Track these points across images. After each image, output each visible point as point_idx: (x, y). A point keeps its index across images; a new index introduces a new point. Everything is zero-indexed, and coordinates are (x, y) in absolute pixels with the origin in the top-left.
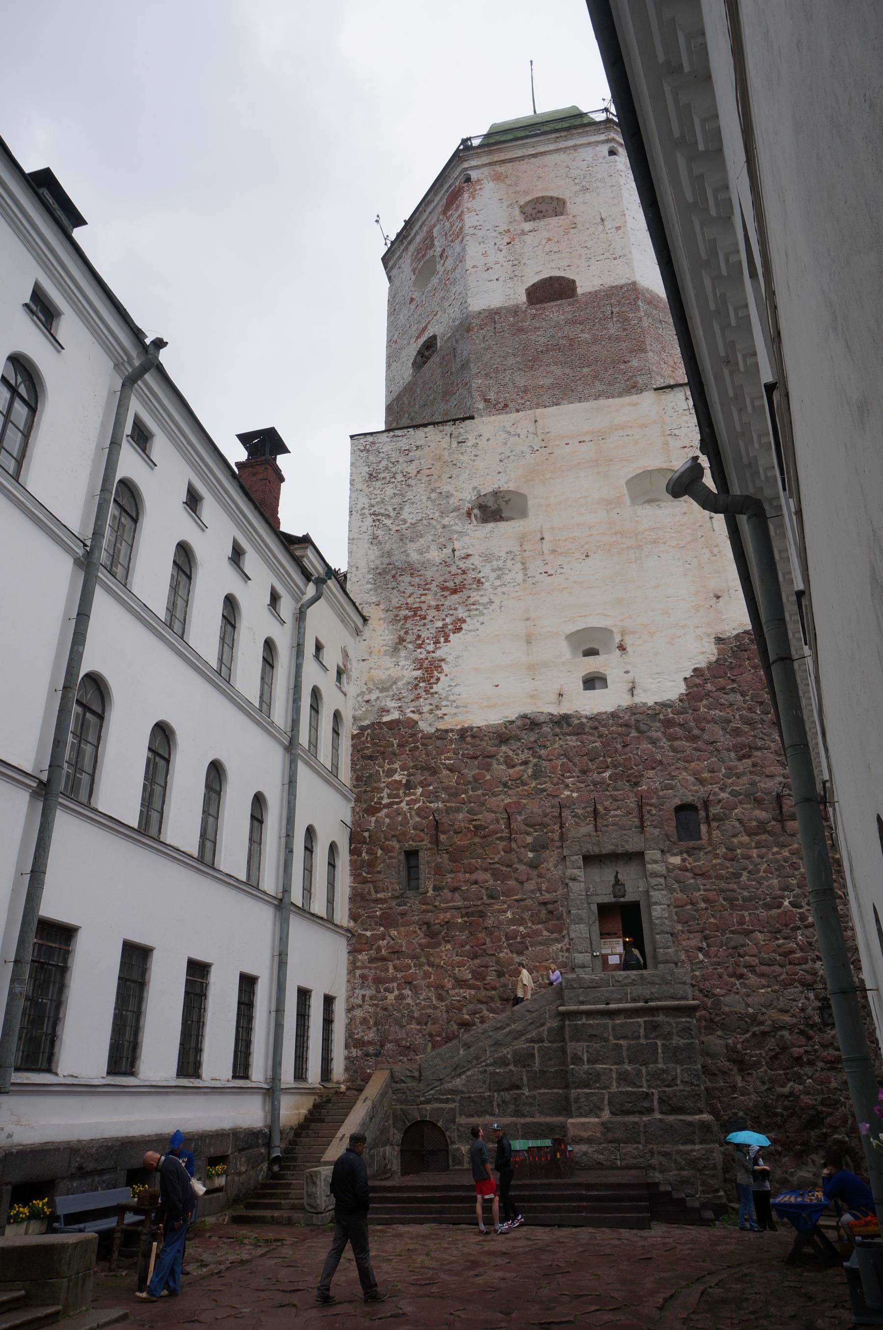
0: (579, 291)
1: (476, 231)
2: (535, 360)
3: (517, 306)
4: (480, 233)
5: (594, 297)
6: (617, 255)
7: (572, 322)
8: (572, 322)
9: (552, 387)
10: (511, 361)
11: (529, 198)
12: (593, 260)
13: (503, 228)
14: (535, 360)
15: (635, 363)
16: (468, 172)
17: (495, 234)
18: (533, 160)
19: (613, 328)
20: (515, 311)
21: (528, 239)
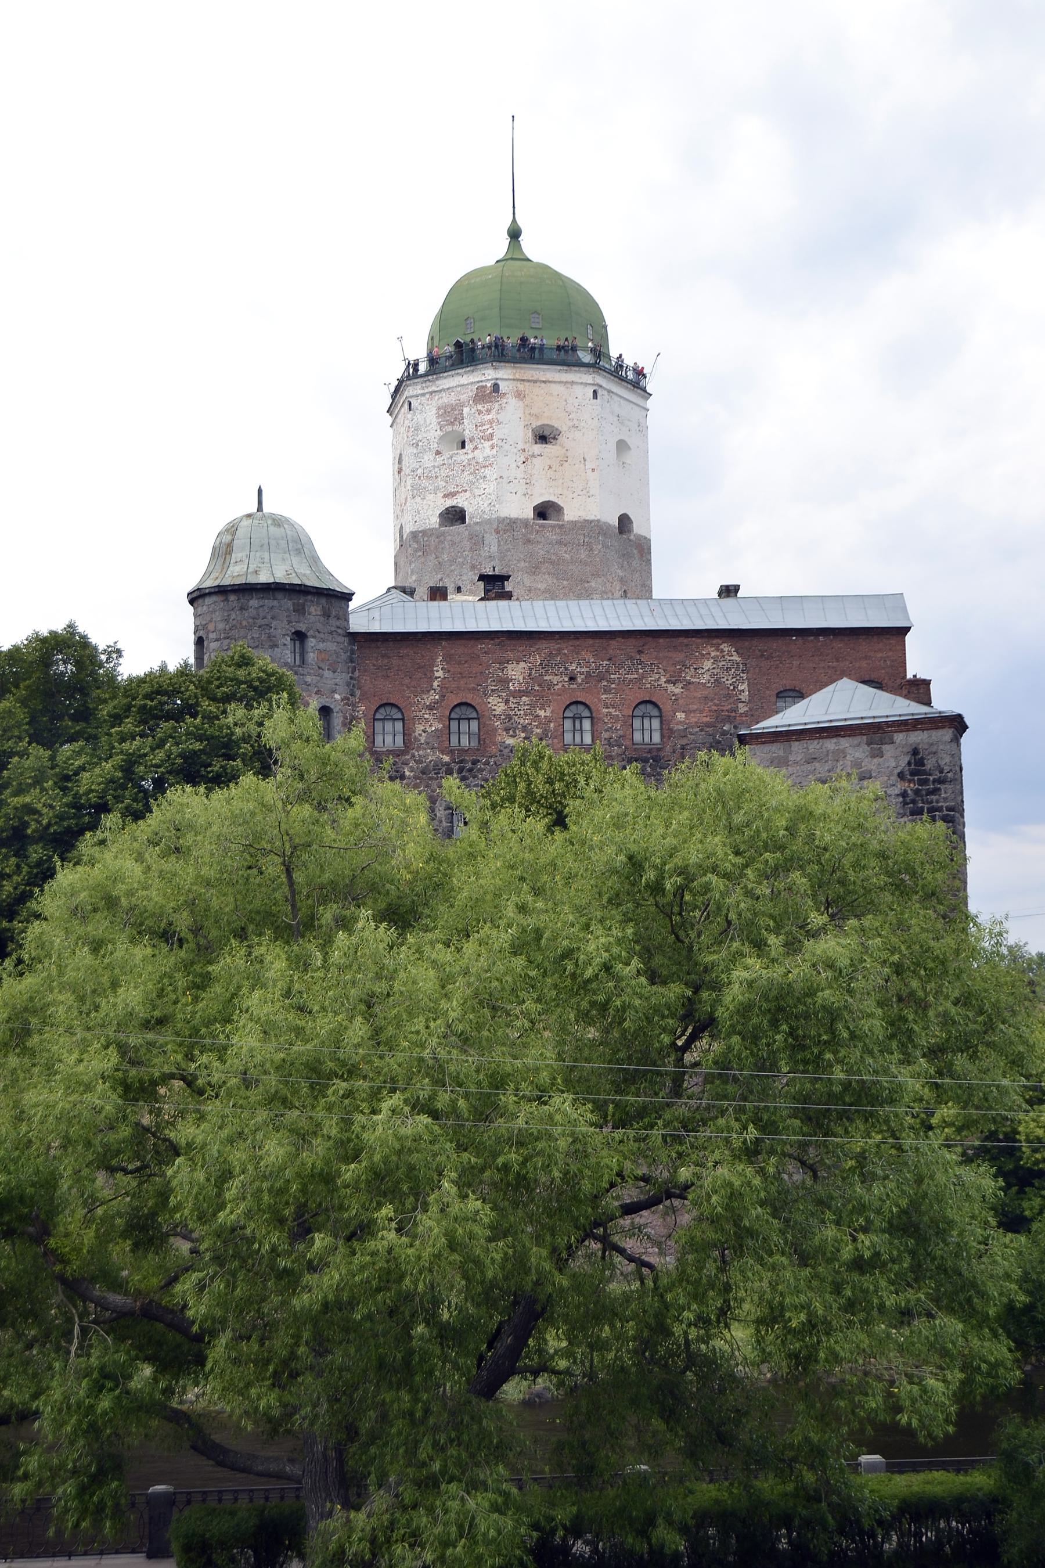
0: (566, 518)
1: (503, 444)
2: (536, 568)
3: (527, 520)
4: (506, 447)
5: (574, 523)
6: (591, 493)
7: (560, 542)
8: (560, 542)
9: (546, 591)
10: (522, 564)
11: (539, 423)
12: (575, 495)
13: (521, 446)
14: (536, 568)
15: (593, 584)
16: (499, 382)
17: (515, 451)
18: (543, 385)
19: (583, 555)
20: (525, 523)
21: (537, 461)
